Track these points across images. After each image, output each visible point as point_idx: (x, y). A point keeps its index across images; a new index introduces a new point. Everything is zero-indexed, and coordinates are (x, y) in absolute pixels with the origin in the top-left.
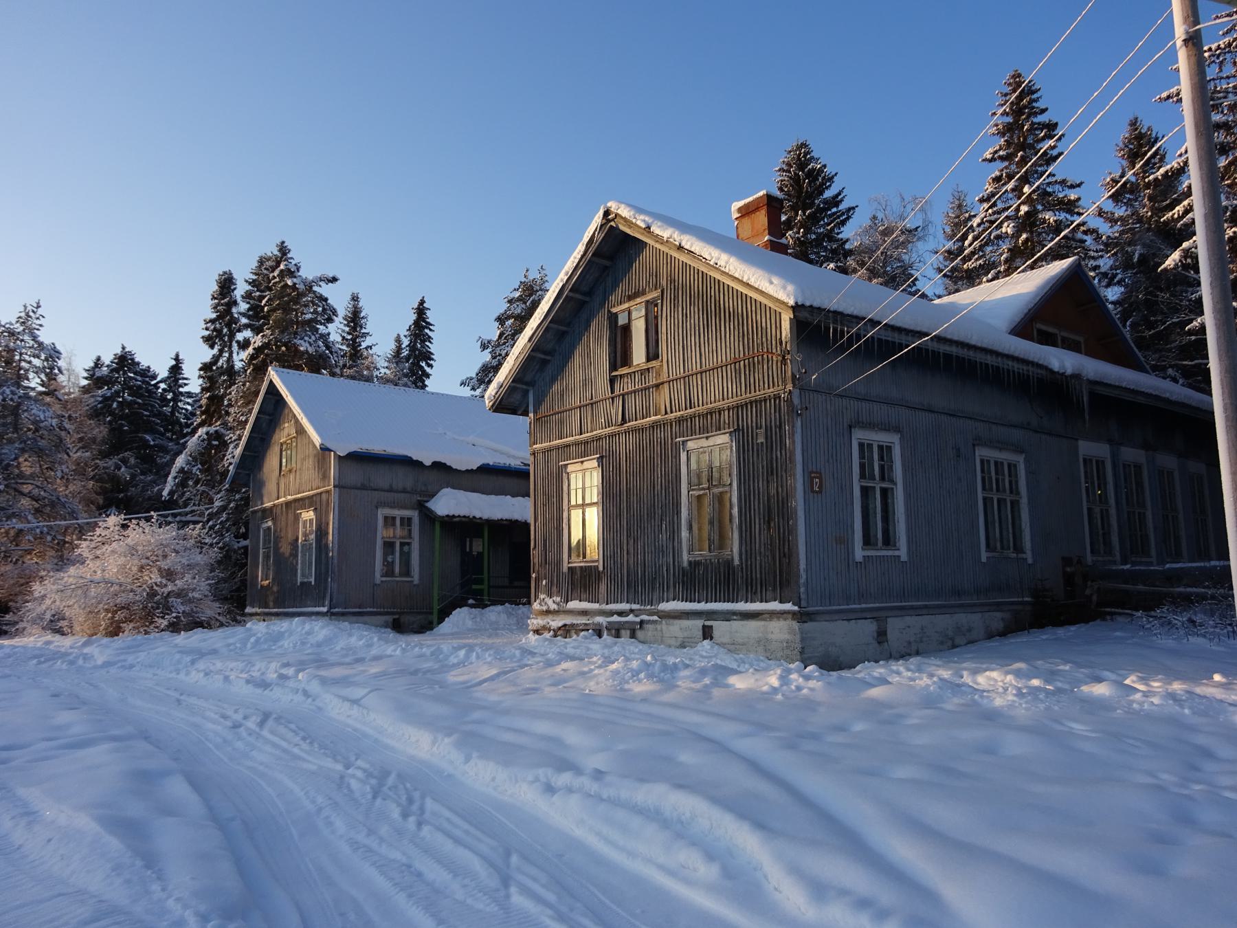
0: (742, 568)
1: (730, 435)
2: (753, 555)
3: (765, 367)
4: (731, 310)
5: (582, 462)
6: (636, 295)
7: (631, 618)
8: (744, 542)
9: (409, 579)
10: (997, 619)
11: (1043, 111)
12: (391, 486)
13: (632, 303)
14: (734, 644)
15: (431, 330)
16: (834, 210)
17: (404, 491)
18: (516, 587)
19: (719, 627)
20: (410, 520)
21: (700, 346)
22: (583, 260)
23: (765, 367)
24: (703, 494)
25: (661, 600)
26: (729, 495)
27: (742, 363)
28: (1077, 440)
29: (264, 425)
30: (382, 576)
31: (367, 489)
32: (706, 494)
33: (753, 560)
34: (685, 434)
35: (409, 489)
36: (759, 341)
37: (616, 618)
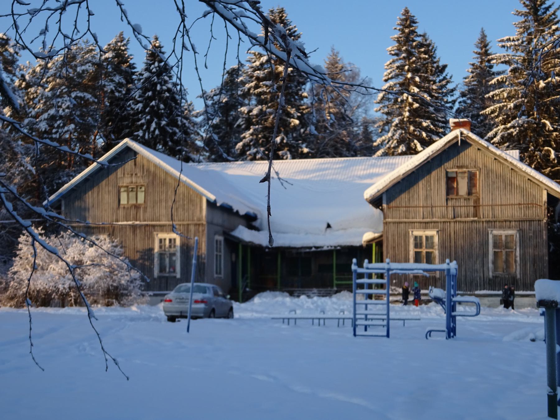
6: (462, 167)
13: (460, 170)
25: (477, 290)
26: (514, 253)
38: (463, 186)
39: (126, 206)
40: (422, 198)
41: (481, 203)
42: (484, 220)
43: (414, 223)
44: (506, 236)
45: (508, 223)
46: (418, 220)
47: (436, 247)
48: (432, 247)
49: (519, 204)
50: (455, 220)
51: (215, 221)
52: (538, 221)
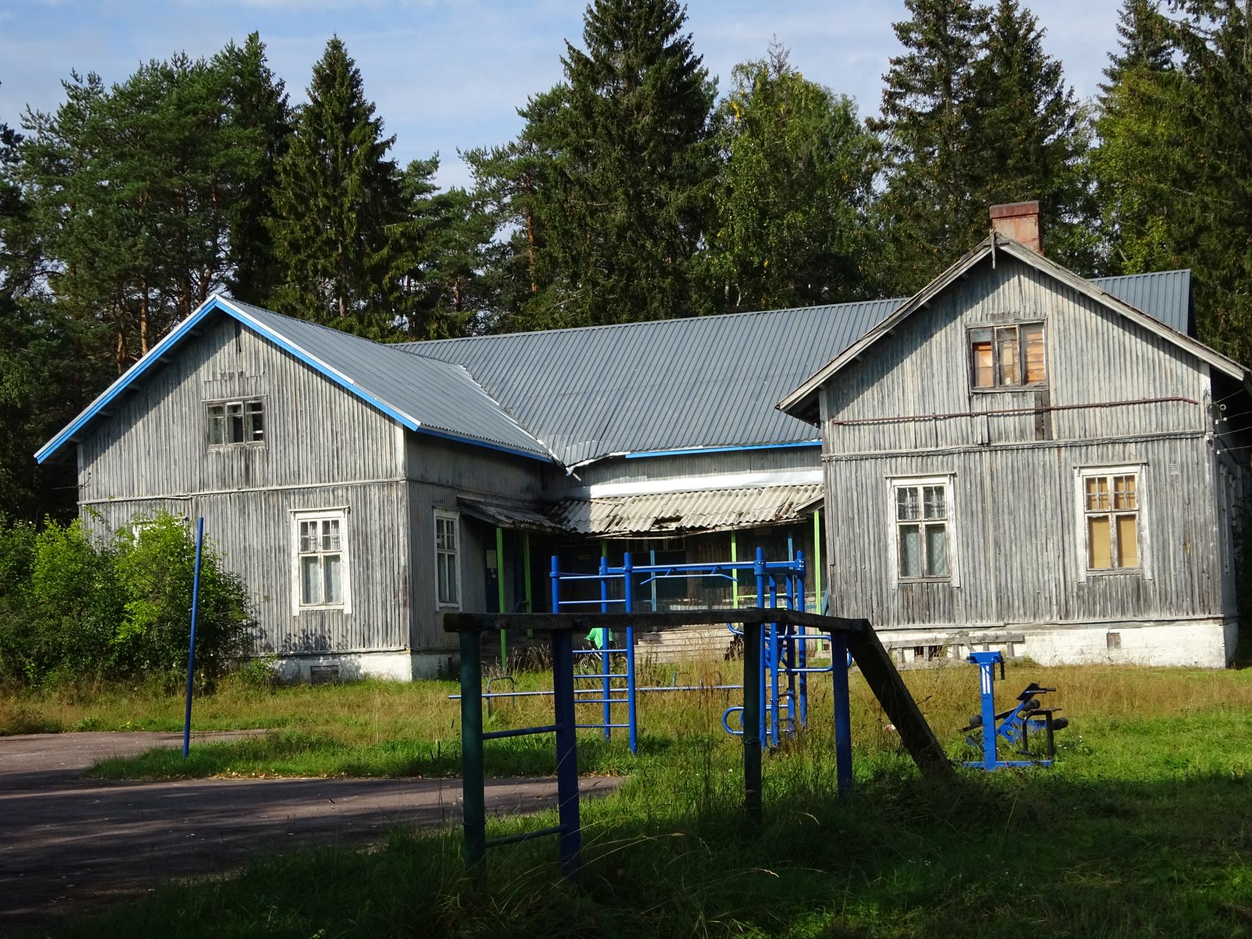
3: (1181, 410)
4: (1140, 354)
8: (1155, 559)
33: (1167, 575)
40: (911, 397)
41: (1053, 404)
42: (1062, 442)
45: (1118, 448)
51: (434, 477)
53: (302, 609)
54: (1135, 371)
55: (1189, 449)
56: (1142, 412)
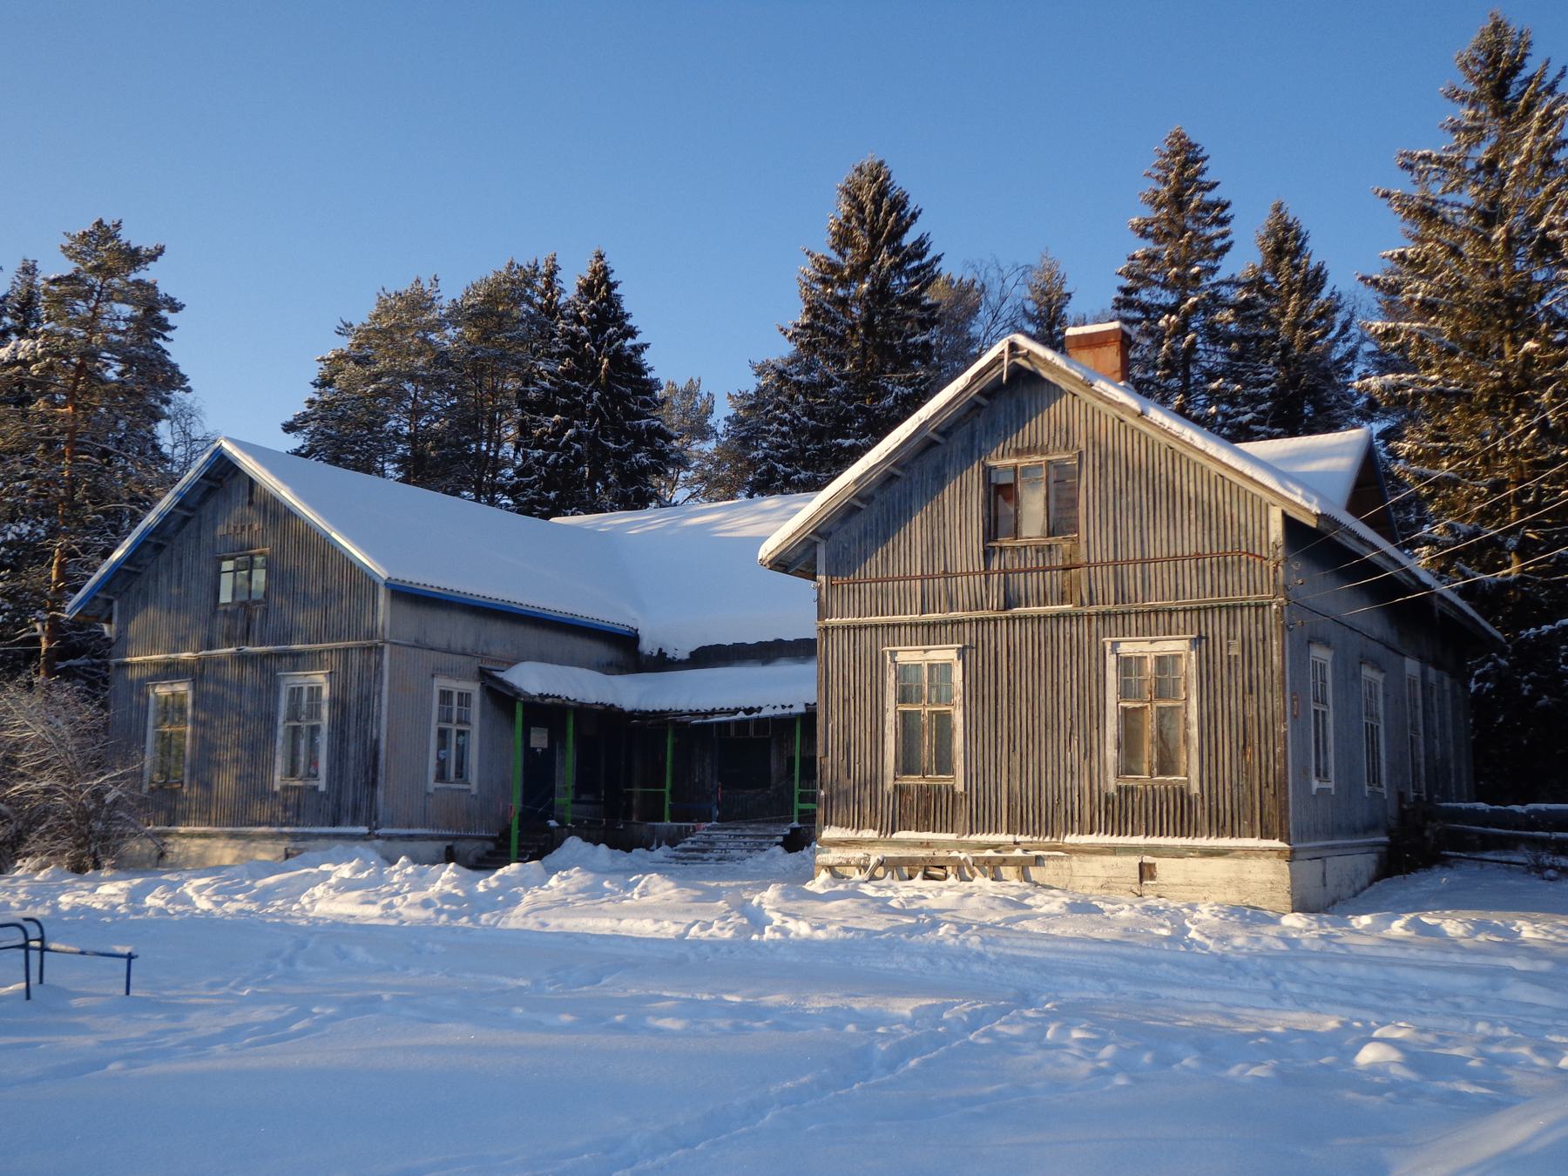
0: (1203, 798)
1: (1191, 643)
2: (1220, 784)
3: (1243, 569)
4: (1192, 495)
5: (926, 651)
6: (1030, 450)
7: (1018, 853)
9: (465, 787)
10: (1365, 863)
11: (1214, 185)
12: (449, 646)
13: (1024, 462)
14: (1190, 885)
15: (165, 338)
16: (915, 264)
17: (464, 654)
18: (583, 802)
19: (1164, 866)
20: (468, 695)
21: (1141, 531)
22: (964, 396)
23: (1243, 569)
24: (1142, 708)
25: (1069, 830)
27: (1207, 560)
28: (1404, 656)
29: (171, 525)
30: (436, 781)
31: (422, 648)
32: (1146, 707)
33: (1220, 789)
34: (1114, 633)
35: (469, 651)
36: (1236, 539)
37: (990, 853)
38: (1033, 508)
39: (229, 608)
42: (1093, 609)
43: (899, 625)
44: (1160, 660)
46: (907, 618)
47: (958, 699)
48: (949, 702)
49: (1198, 556)
50: (1008, 613)
51: (439, 639)
52: (1257, 606)
53: (285, 783)
54: (1186, 517)
55: (1253, 620)
56: (1194, 572)
